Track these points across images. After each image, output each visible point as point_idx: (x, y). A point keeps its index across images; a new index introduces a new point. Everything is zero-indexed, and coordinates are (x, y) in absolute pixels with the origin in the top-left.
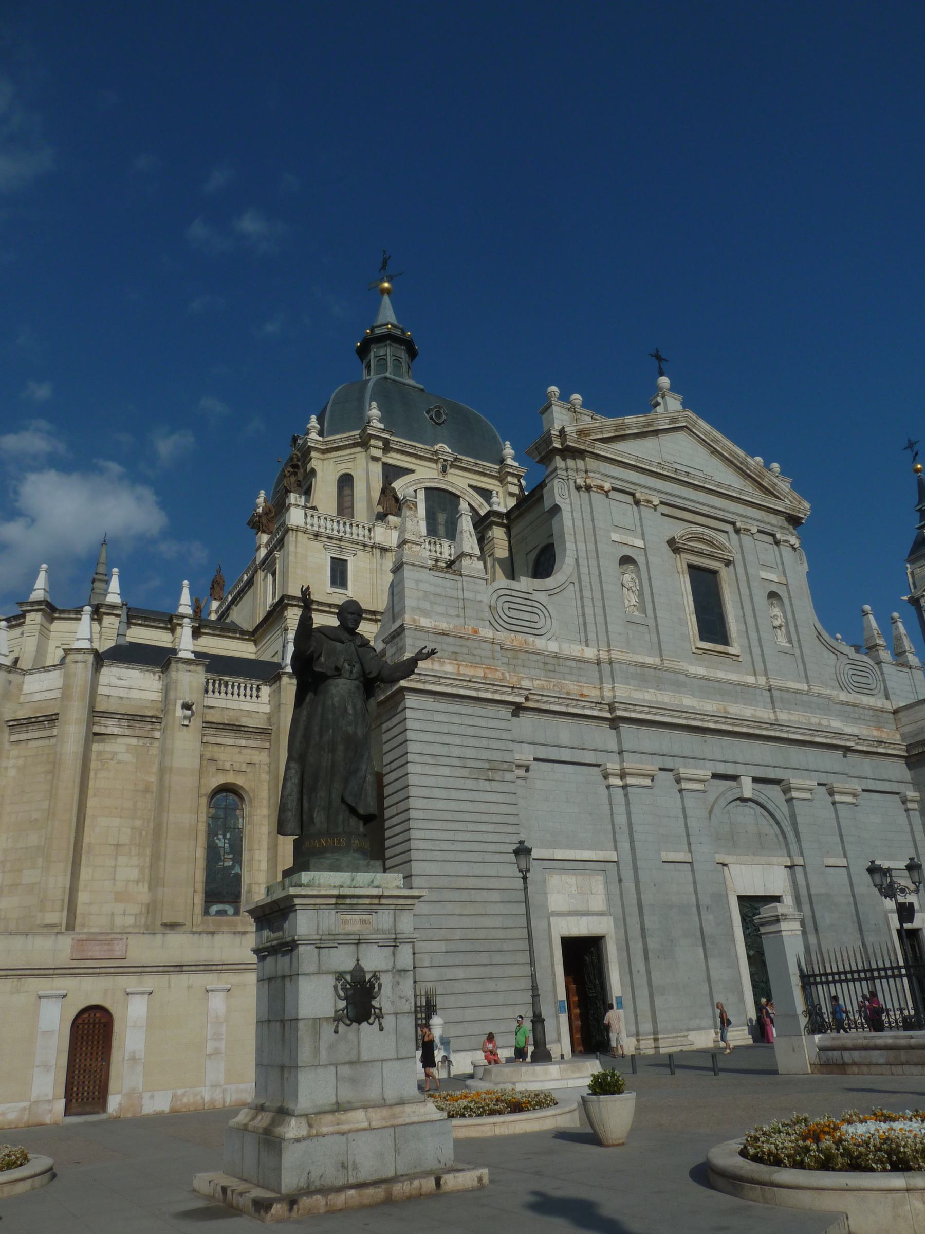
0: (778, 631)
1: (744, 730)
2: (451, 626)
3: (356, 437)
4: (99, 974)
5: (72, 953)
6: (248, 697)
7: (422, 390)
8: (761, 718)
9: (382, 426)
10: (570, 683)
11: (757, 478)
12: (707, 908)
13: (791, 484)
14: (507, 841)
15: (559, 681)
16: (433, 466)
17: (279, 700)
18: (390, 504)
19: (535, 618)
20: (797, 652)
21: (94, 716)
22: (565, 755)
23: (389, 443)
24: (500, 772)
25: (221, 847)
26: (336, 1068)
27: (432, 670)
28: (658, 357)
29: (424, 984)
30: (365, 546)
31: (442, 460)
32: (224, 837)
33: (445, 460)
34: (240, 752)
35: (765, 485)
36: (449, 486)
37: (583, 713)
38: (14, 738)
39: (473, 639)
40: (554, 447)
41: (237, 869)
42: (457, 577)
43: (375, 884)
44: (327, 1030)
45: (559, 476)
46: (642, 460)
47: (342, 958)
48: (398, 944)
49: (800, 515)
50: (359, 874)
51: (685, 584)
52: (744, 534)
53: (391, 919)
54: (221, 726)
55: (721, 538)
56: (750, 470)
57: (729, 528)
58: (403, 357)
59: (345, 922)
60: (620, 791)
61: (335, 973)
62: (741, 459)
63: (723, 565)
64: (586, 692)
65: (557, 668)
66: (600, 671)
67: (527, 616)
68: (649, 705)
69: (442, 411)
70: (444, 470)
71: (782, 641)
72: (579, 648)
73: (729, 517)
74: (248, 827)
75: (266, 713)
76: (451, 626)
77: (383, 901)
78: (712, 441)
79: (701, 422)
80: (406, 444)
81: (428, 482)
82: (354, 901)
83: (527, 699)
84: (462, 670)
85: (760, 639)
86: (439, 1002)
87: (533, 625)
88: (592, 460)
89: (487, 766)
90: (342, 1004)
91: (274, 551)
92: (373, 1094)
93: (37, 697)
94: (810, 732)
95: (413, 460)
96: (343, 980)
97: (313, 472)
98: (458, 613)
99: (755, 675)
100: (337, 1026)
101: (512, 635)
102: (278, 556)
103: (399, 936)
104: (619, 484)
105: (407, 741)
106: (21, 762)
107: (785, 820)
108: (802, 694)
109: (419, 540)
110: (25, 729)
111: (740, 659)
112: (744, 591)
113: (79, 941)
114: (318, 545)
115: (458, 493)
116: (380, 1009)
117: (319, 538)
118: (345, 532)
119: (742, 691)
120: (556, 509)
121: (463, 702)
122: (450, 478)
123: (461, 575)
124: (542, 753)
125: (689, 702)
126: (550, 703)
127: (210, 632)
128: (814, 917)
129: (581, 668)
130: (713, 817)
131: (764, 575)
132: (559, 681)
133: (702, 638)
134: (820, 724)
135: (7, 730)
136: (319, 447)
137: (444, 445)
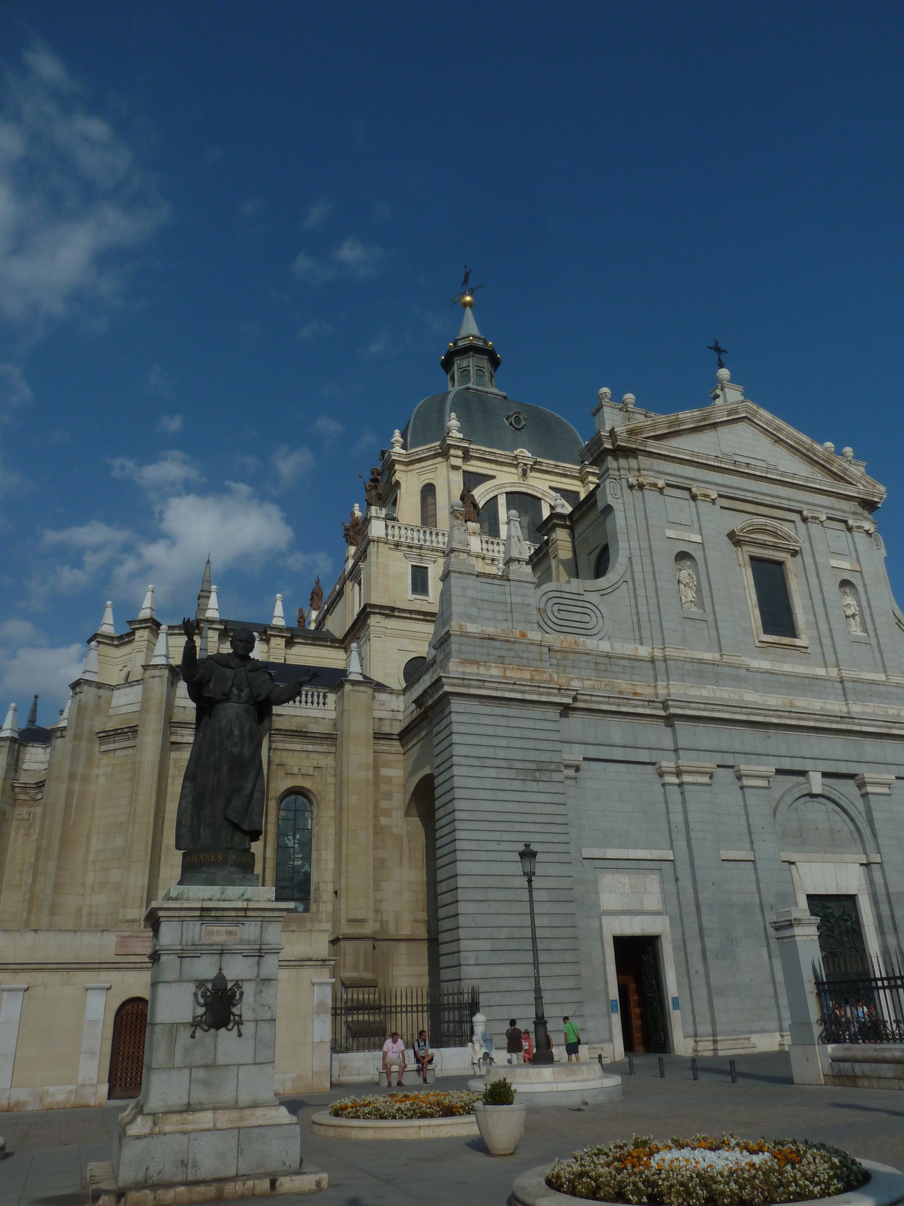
0: (852, 620)
1: (811, 724)
2: (499, 630)
3: (437, 448)
4: (141, 968)
5: (116, 949)
6: (315, 704)
7: (505, 397)
8: (832, 711)
9: (461, 436)
10: (622, 681)
11: (825, 464)
12: (772, 908)
13: (865, 468)
14: (555, 841)
15: (611, 680)
16: (514, 470)
17: (343, 706)
18: (468, 511)
19: (586, 618)
20: (874, 641)
21: (171, 727)
22: (618, 754)
23: (469, 451)
24: (548, 773)
25: (291, 847)
26: (191, 1070)
27: (478, 674)
28: (718, 350)
29: (469, 982)
31: (522, 465)
32: (294, 838)
33: (525, 464)
34: (308, 757)
35: (835, 470)
36: (530, 489)
37: (635, 712)
38: (104, 748)
39: (520, 643)
40: (605, 448)
41: (306, 868)
42: (505, 582)
43: (246, 897)
44: (184, 1035)
45: (611, 476)
46: (697, 455)
47: (205, 968)
48: (263, 954)
49: (875, 499)
50: (229, 887)
51: (748, 577)
52: (812, 522)
53: (258, 931)
54: (289, 733)
55: (787, 528)
56: (818, 457)
57: (796, 517)
58: (485, 366)
59: (211, 933)
60: (677, 789)
61: (196, 981)
62: (807, 446)
64: (639, 690)
65: (609, 667)
66: (654, 669)
67: (577, 617)
68: (705, 702)
69: (521, 417)
72: (632, 646)
73: (795, 506)
74: (316, 829)
75: (332, 719)
76: (499, 630)
77: (250, 913)
78: (775, 429)
79: (762, 412)
80: (485, 451)
81: (508, 487)
82: (219, 914)
83: (575, 699)
84: (508, 673)
85: (830, 630)
86: (483, 999)
87: (584, 626)
88: (646, 458)
89: (534, 766)
90: (201, 1011)
91: (359, 562)
92: (227, 1095)
93: (123, 710)
94: (886, 724)
95: (493, 466)
96: (204, 988)
97: (398, 484)
98: (505, 618)
99: (826, 666)
100: (194, 1032)
101: (562, 637)
102: (362, 566)
103: (263, 947)
104: (673, 480)
105: (452, 744)
106: (109, 769)
107: (860, 816)
108: (879, 684)
109: (466, 548)
110: (112, 740)
111: (809, 651)
112: (813, 580)
113: (122, 937)
114: (398, 554)
115: (539, 495)
116: (240, 1016)
117: (399, 548)
118: (425, 541)
119: (811, 684)
120: (608, 509)
121: (510, 705)
122: (530, 481)
123: (509, 580)
124: (593, 752)
125: (750, 697)
126: (600, 703)
127: (303, 641)
128: (893, 917)
129: (634, 667)
130: (778, 815)
131: (834, 563)
132: (611, 680)
133: (766, 631)
134: (898, 716)
135: (97, 741)
136: (403, 460)
137: (523, 450)
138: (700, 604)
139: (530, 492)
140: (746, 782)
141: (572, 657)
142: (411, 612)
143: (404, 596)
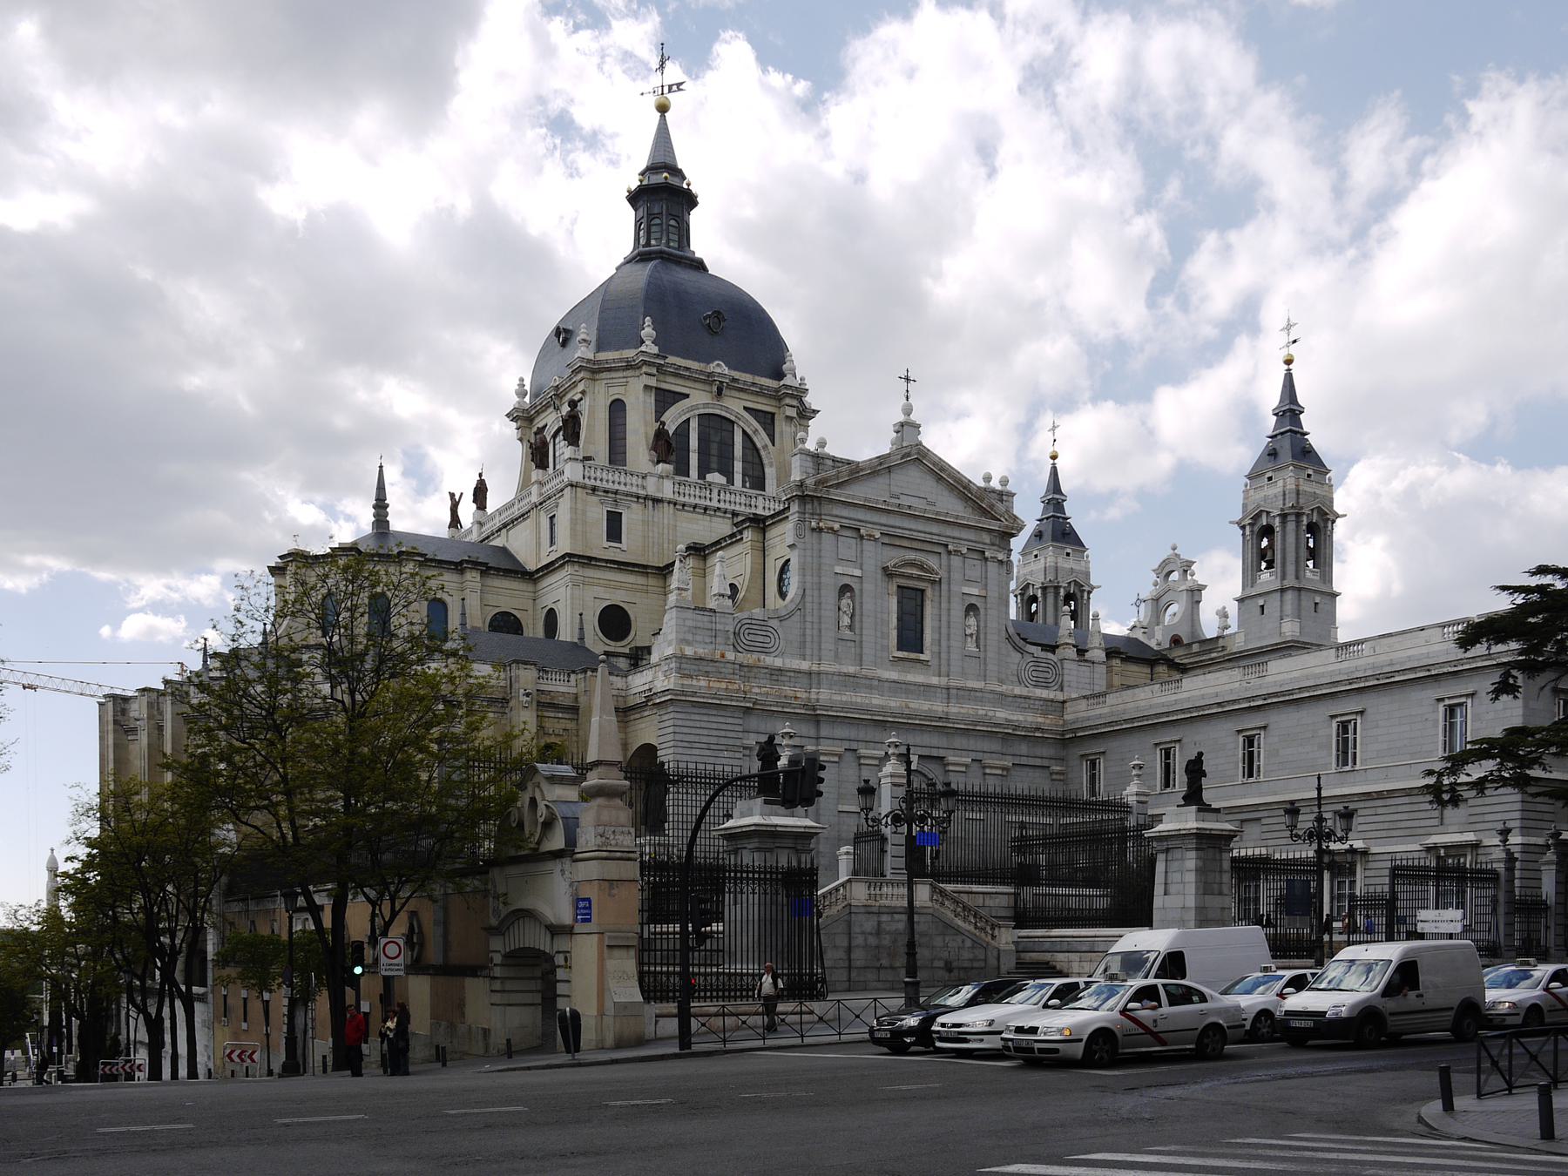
0: (969, 639)
19: (768, 640)
30: (638, 498)
55: (932, 562)
57: (940, 549)
63: (929, 585)
67: (761, 639)
71: (971, 646)
72: (797, 662)
73: (943, 540)
83: (754, 703)
85: (949, 647)
87: (766, 645)
112: (944, 605)
114: (594, 499)
115: (733, 418)
125: (877, 701)
131: (966, 590)
133: (899, 649)
138: (851, 627)
139: (724, 414)
140: (862, 761)
141: (755, 670)
142: (607, 561)
143: (599, 546)
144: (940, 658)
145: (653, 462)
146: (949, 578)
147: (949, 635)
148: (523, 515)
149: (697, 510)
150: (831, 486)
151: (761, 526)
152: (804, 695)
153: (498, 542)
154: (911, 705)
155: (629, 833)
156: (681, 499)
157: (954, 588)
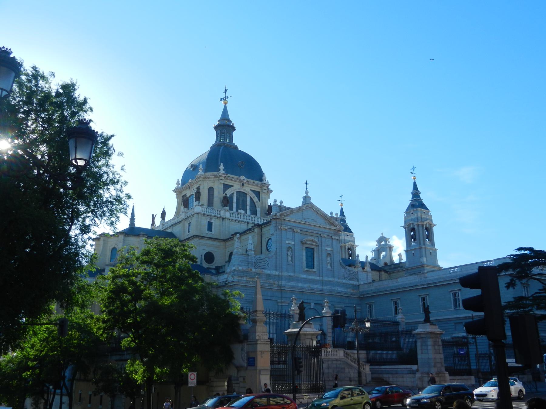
0: (328, 264)
16: (239, 183)
19: (265, 265)
28: (307, 184)
30: (218, 217)
57: (318, 235)
64: (275, 283)
70: (243, 185)
71: (329, 267)
73: (319, 233)
76: (246, 268)
85: (322, 267)
95: (233, 182)
114: (204, 218)
115: (247, 193)
131: (327, 248)
133: (307, 268)
139: (244, 191)
143: (205, 232)
144: (319, 270)
145: (222, 206)
146: (321, 245)
147: (322, 263)
148: (179, 222)
149: (236, 221)
150: (284, 216)
151: (261, 227)
152: (277, 283)
153: (169, 230)
154: (311, 286)
155: (267, 335)
156: (231, 218)
157: (323, 248)
